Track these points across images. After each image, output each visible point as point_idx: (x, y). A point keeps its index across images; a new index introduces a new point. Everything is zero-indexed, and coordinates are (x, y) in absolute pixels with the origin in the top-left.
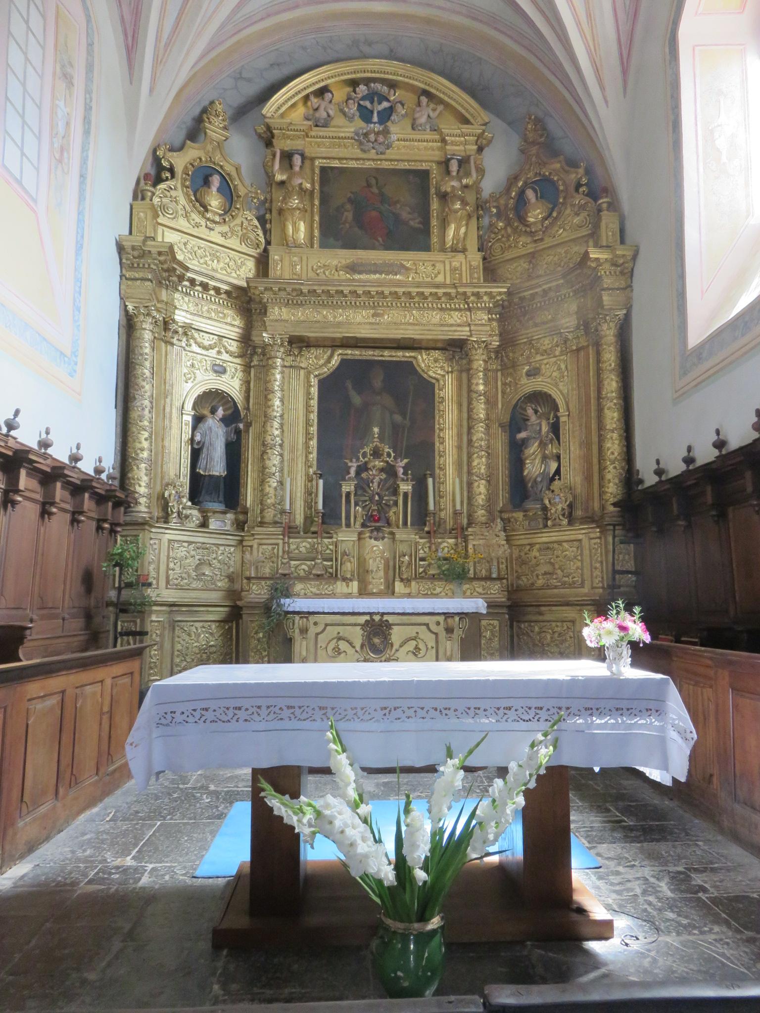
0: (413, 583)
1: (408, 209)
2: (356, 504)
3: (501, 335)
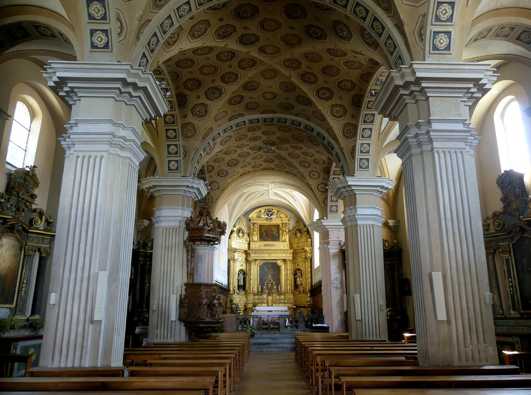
3: (293, 257)
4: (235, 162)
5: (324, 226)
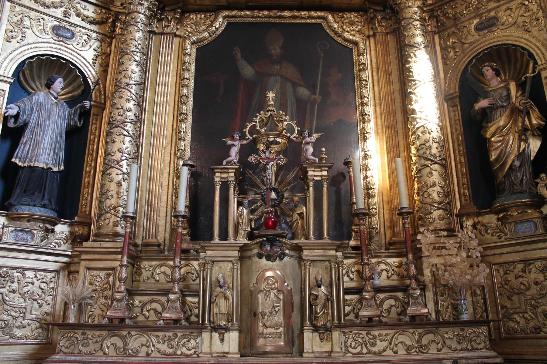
0: (336, 334)
2: (240, 204)
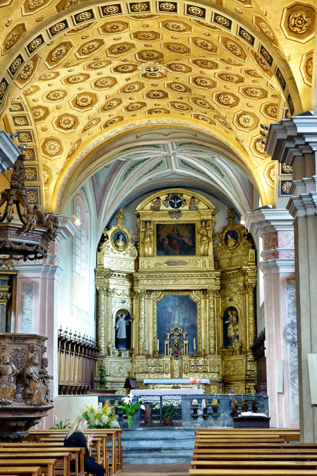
0: (189, 374)
1: (188, 239)
2: (170, 347)
3: (220, 285)
4: (90, 99)
5: (268, 221)
